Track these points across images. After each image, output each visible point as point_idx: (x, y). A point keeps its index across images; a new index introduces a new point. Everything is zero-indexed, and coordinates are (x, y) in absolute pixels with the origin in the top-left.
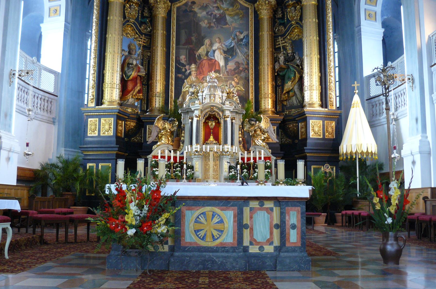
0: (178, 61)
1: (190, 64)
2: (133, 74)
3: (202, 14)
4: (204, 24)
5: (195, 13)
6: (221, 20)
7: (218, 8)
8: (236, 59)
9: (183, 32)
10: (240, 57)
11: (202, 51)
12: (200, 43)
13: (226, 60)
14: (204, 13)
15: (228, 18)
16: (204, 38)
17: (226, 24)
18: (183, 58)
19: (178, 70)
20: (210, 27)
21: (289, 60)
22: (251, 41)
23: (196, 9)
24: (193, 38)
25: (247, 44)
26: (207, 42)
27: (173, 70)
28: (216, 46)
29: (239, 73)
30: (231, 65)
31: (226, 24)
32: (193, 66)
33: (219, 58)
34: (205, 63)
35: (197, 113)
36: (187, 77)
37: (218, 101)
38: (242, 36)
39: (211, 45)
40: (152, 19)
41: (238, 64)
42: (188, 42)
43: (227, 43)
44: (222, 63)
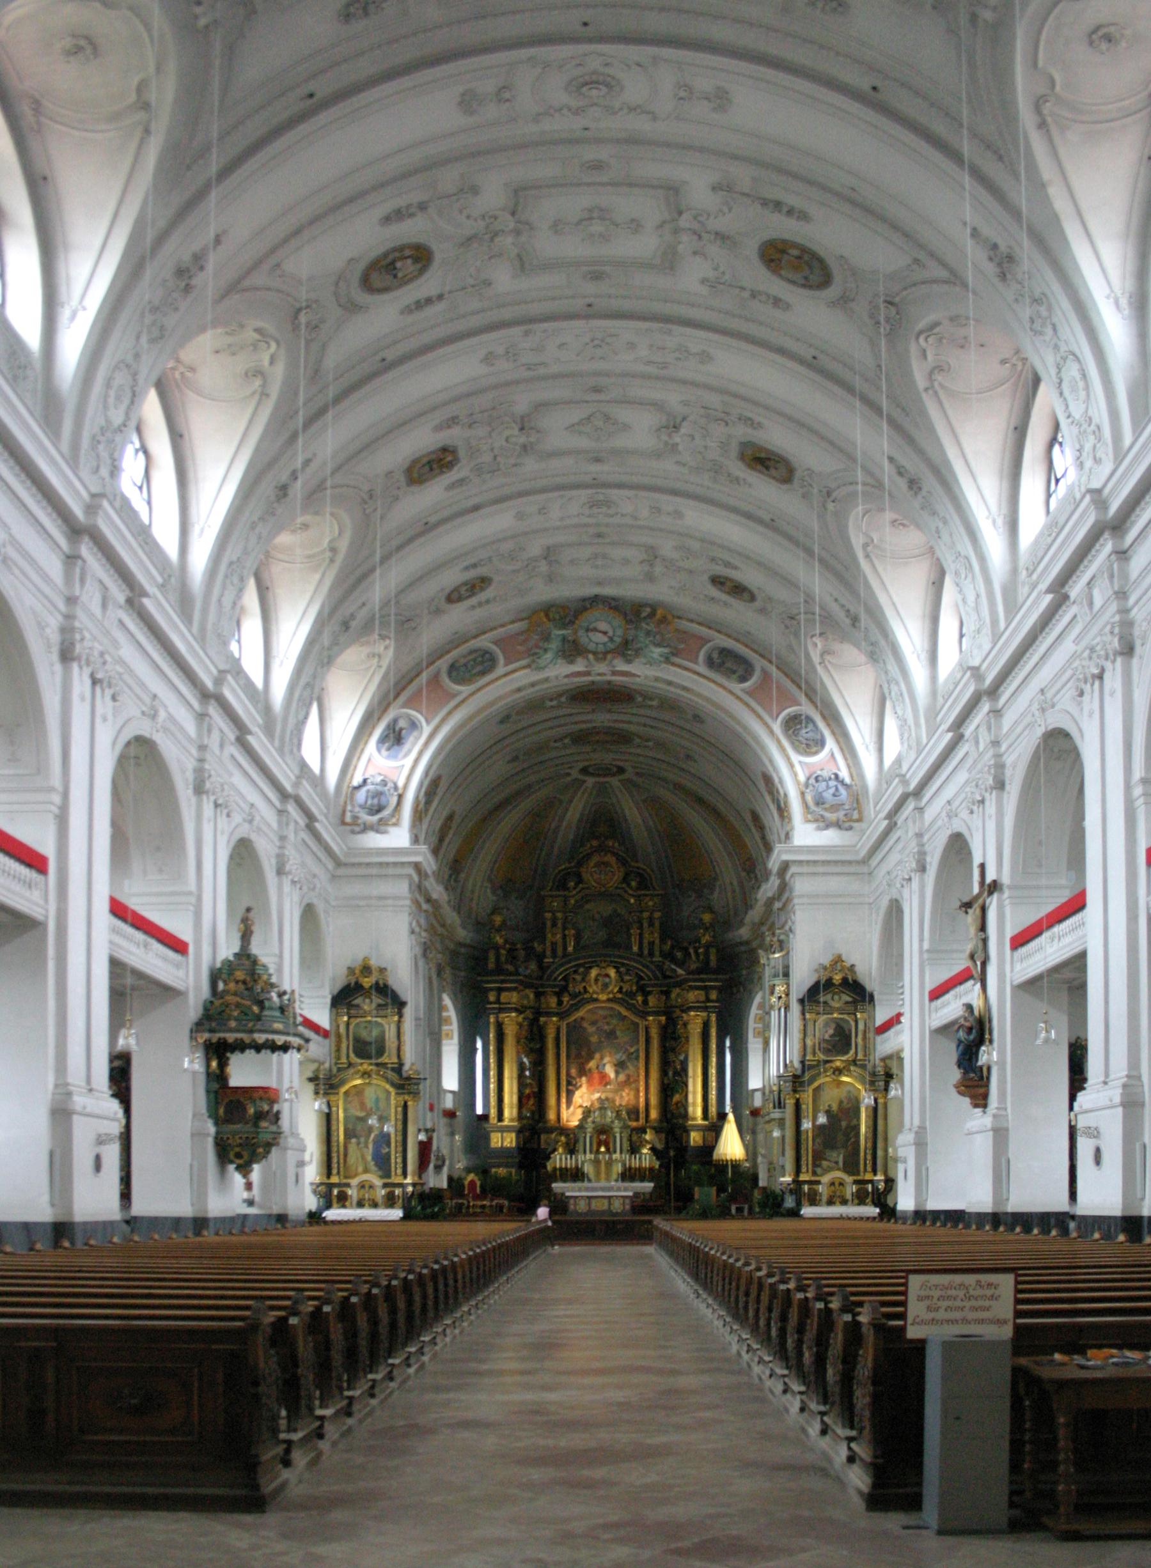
0: (568, 1074)
1: (580, 1077)
2: (527, 1091)
3: (591, 1029)
4: (594, 1039)
5: (585, 1029)
6: (611, 1035)
7: (608, 1023)
8: (627, 1072)
9: (573, 1047)
10: (631, 1069)
11: (592, 1064)
12: (590, 1057)
13: (617, 1073)
14: (594, 1029)
15: (618, 1033)
16: (594, 1053)
17: (616, 1038)
18: (573, 1072)
19: (569, 1083)
20: (600, 1042)
21: (676, 1073)
22: (642, 1055)
23: (585, 1025)
24: (583, 1053)
25: (637, 1058)
26: (597, 1056)
27: (564, 1083)
28: (606, 1060)
29: (630, 1084)
30: (622, 1077)
31: (616, 1038)
32: (584, 1079)
33: (610, 1071)
34: (596, 1076)
35: (589, 1130)
36: (577, 1089)
37: (609, 1120)
38: (632, 1050)
39: (602, 1058)
40: (542, 1038)
41: (628, 1076)
42: (579, 1056)
43: (618, 1056)
44: (612, 1075)
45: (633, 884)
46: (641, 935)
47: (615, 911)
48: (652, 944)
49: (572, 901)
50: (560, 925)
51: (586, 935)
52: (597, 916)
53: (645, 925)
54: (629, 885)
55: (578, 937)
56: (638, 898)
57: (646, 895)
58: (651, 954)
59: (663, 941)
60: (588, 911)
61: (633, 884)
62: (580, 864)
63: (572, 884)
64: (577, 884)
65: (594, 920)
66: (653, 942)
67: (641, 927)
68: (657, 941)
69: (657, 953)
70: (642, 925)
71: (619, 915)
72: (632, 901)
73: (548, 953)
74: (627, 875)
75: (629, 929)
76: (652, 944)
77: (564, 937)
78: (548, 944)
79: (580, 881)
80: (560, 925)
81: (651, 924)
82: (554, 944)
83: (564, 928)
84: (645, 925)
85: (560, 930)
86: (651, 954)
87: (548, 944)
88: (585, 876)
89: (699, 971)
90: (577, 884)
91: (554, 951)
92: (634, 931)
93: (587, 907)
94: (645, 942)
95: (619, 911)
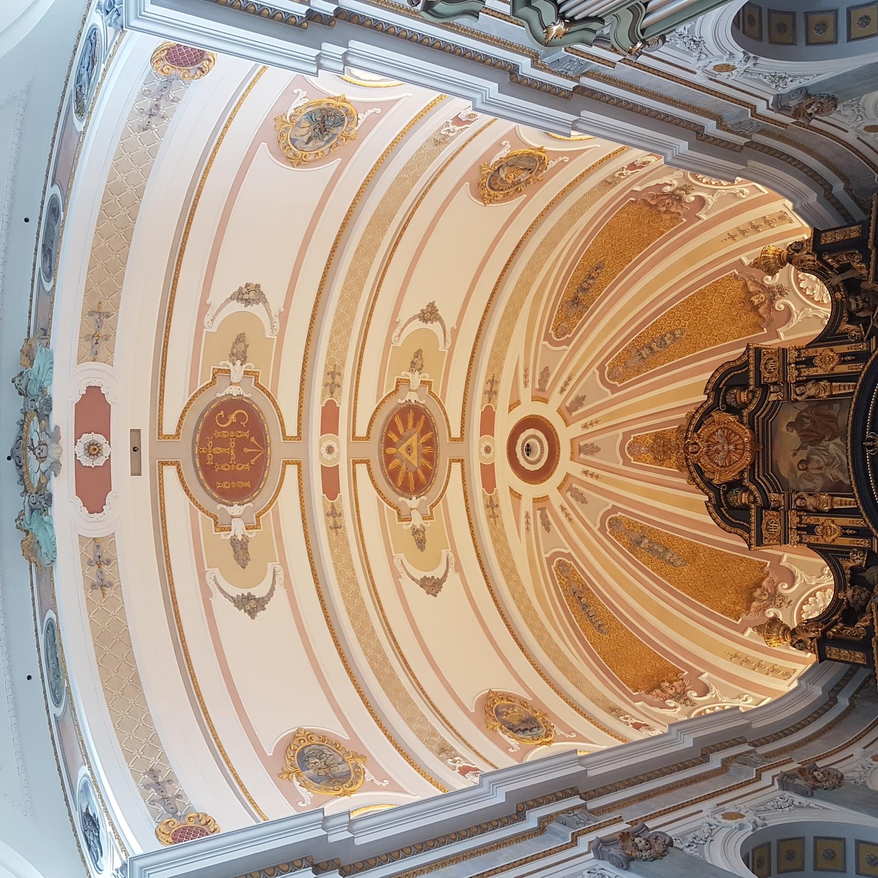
45: (744, 397)
46: (832, 378)
47: (790, 424)
48: (843, 359)
49: (773, 496)
50: (812, 520)
51: (834, 474)
52: (802, 455)
53: (807, 372)
54: (745, 405)
55: (836, 489)
56: (765, 388)
57: (758, 373)
58: (859, 357)
59: (843, 338)
60: (792, 471)
61: (744, 397)
62: (709, 483)
63: (744, 498)
64: (746, 489)
65: (806, 462)
66: (843, 355)
67: (818, 379)
68: (844, 349)
69: (863, 347)
70: (809, 379)
71: (799, 418)
72: (773, 397)
73: (864, 543)
74: (730, 410)
75: (824, 402)
76: (843, 359)
77: (833, 512)
78: (846, 542)
79: (735, 485)
80: (812, 520)
81: (809, 362)
82: (845, 532)
83: (819, 512)
84: (812, 372)
85: (822, 519)
86: (859, 357)
87: (846, 542)
88: (730, 477)
89: (866, 260)
90: (746, 489)
91: (860, 533)
92: (822, 391)
93: (784, 472)
94: (844, 368)
95: (792, 419)
